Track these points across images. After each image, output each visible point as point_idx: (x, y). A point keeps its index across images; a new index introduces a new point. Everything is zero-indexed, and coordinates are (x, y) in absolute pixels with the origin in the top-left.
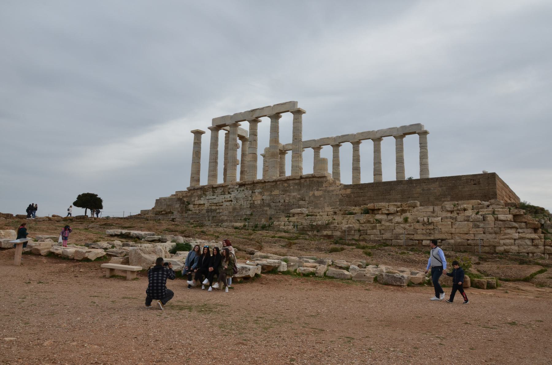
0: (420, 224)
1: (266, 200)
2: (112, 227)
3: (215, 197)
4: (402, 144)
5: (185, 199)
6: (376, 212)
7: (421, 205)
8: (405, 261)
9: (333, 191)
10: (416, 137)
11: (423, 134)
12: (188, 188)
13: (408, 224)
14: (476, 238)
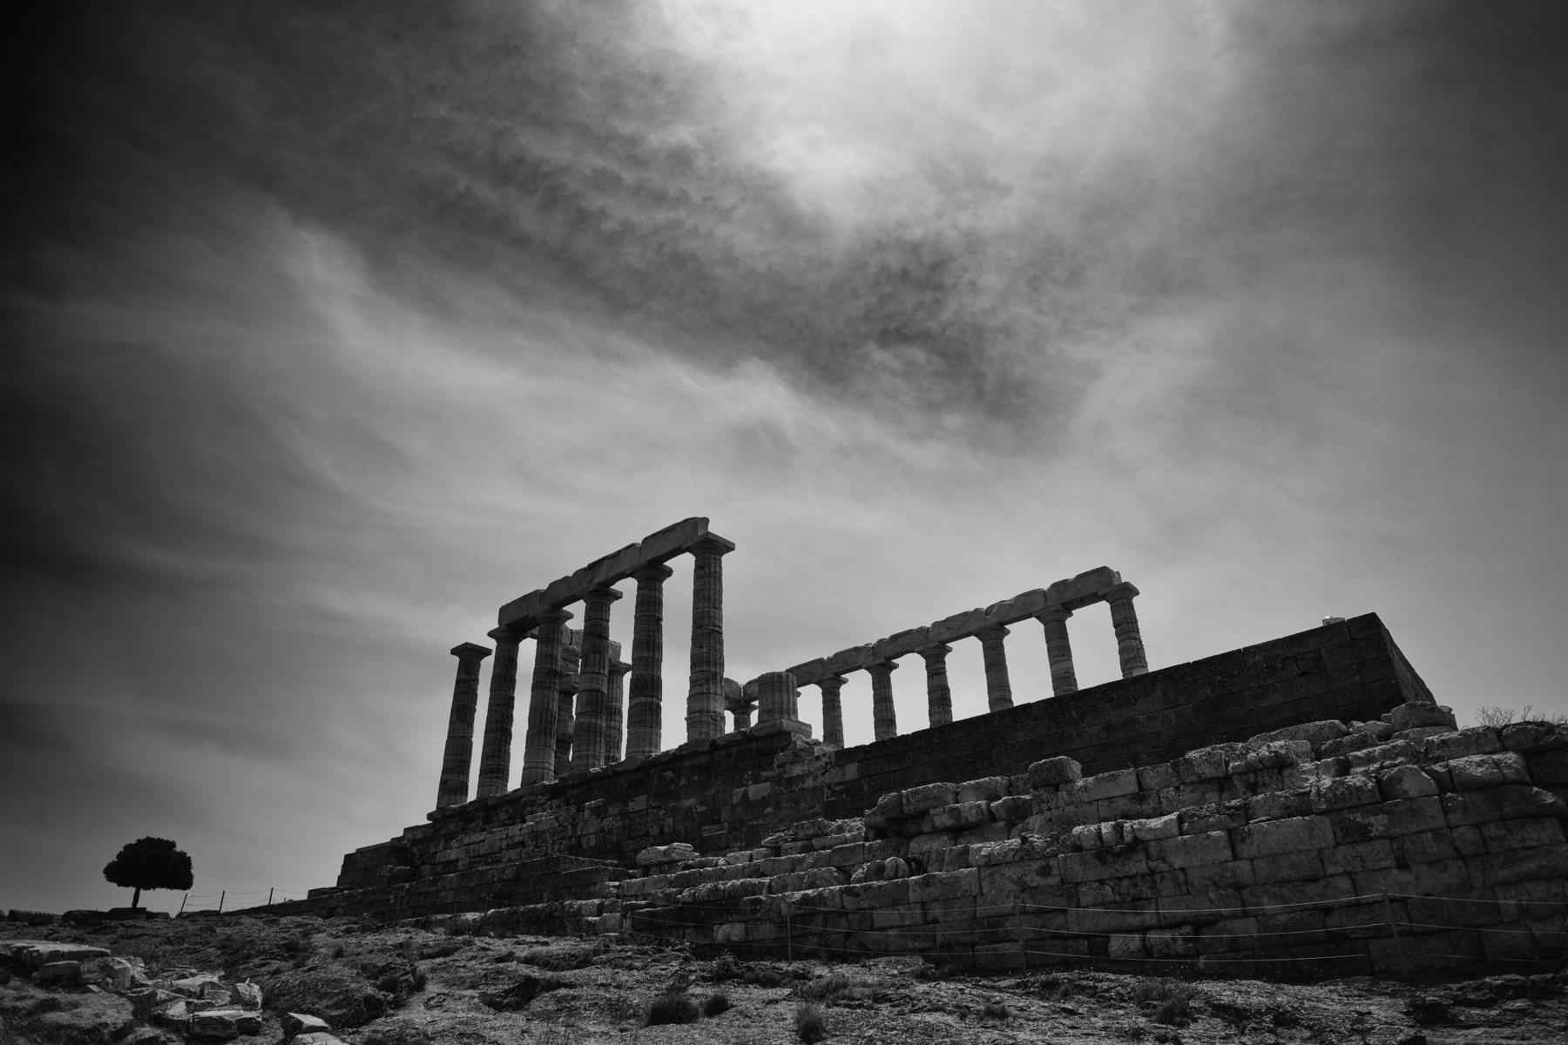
1: (610, 831)
5: (415, 850)
6: (911, 827)
7: (1086, 773)
9: (802, 778)
10: (1102, 609)
12: (430, 816)
13: (1035, 866)
14: (1367, 897)
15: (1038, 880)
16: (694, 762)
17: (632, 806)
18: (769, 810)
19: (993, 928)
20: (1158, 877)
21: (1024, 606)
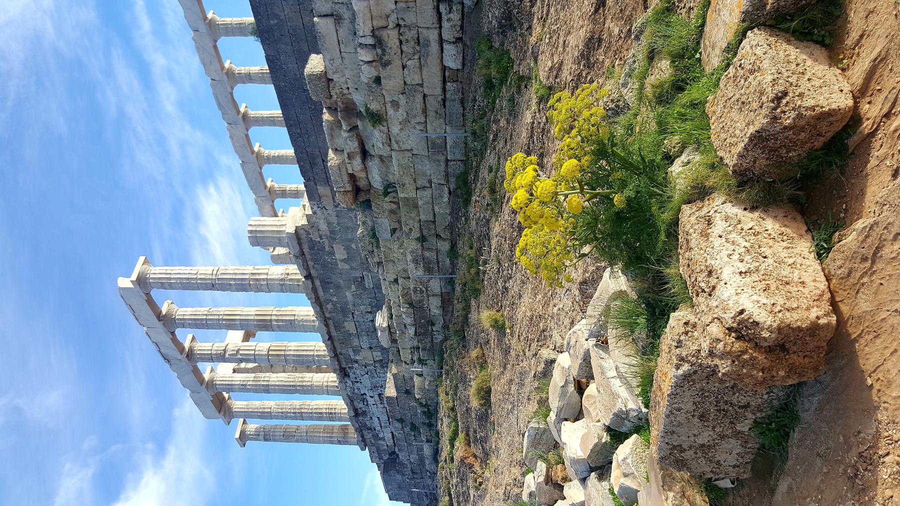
9: (329, 224)
12: (363, 449)
17: (353, 330)
18: (353, 246)
20: (402, 23)
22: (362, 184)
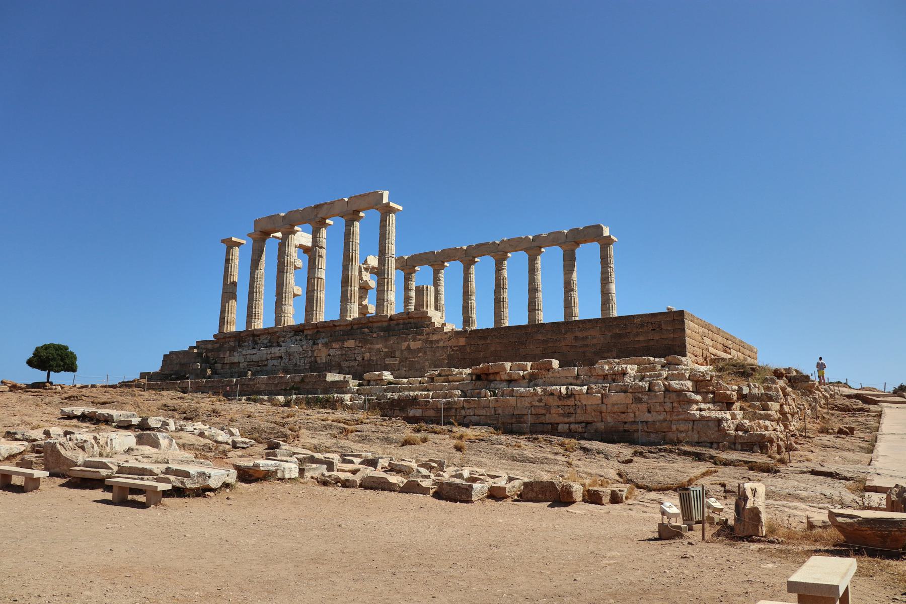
0: (555, 397)
1: (334, 356)
2: (79, 402)
3: (255, 351)
4: (573, 258)
8: (514, 459)
9: (438, 341)
11: (606, 243)
12: (215, 336)
15: (537, 404)
16: (379, 324)
17: (346, 345)
19: (520, 418)
21: (555, 239)
22: (492, 377)
